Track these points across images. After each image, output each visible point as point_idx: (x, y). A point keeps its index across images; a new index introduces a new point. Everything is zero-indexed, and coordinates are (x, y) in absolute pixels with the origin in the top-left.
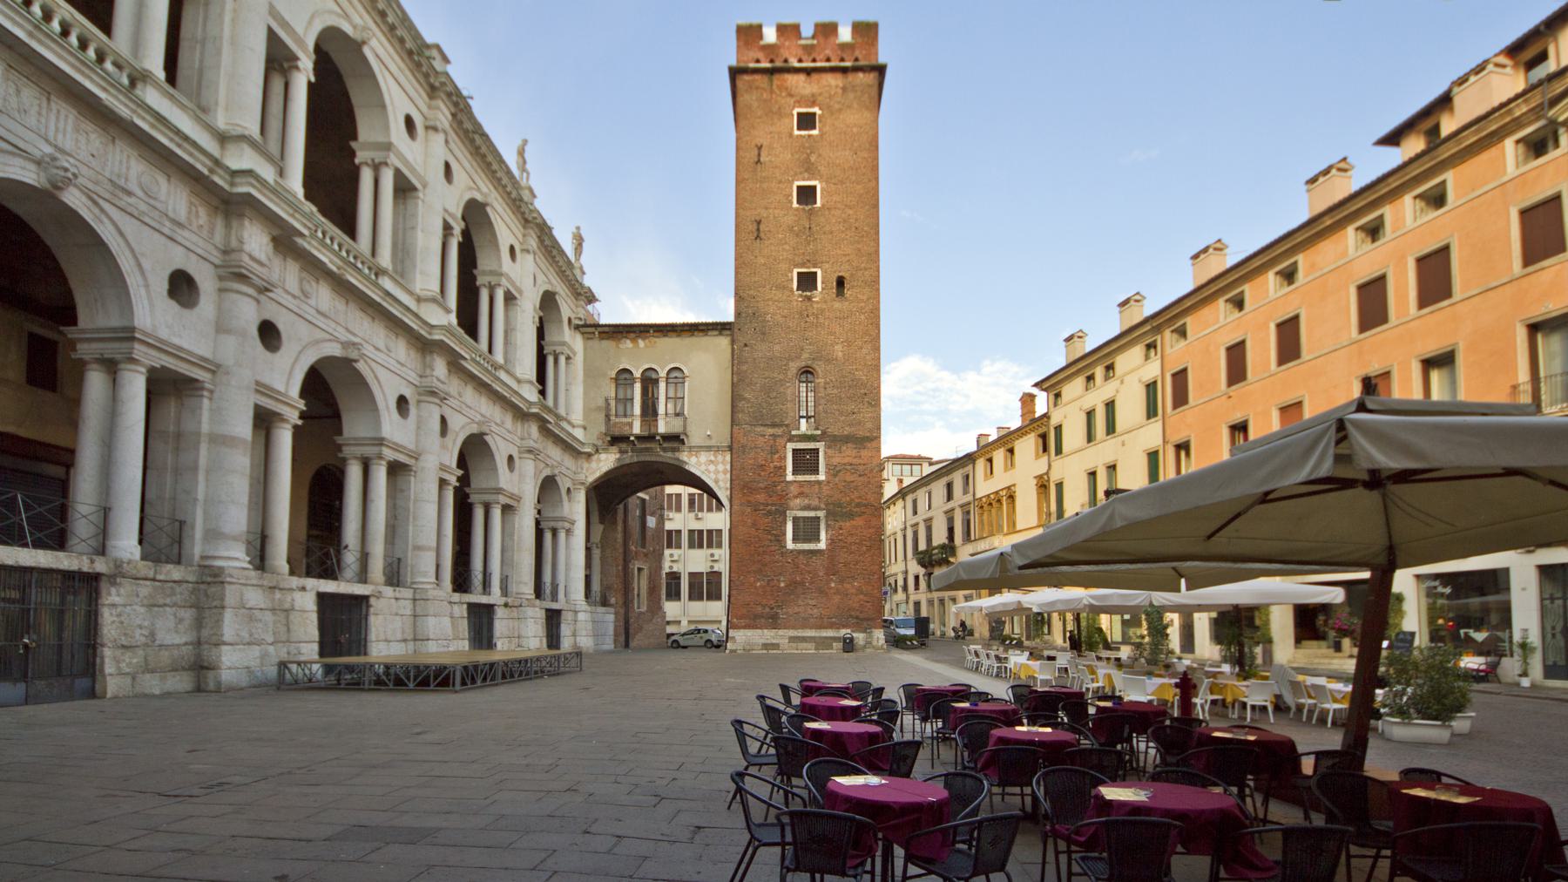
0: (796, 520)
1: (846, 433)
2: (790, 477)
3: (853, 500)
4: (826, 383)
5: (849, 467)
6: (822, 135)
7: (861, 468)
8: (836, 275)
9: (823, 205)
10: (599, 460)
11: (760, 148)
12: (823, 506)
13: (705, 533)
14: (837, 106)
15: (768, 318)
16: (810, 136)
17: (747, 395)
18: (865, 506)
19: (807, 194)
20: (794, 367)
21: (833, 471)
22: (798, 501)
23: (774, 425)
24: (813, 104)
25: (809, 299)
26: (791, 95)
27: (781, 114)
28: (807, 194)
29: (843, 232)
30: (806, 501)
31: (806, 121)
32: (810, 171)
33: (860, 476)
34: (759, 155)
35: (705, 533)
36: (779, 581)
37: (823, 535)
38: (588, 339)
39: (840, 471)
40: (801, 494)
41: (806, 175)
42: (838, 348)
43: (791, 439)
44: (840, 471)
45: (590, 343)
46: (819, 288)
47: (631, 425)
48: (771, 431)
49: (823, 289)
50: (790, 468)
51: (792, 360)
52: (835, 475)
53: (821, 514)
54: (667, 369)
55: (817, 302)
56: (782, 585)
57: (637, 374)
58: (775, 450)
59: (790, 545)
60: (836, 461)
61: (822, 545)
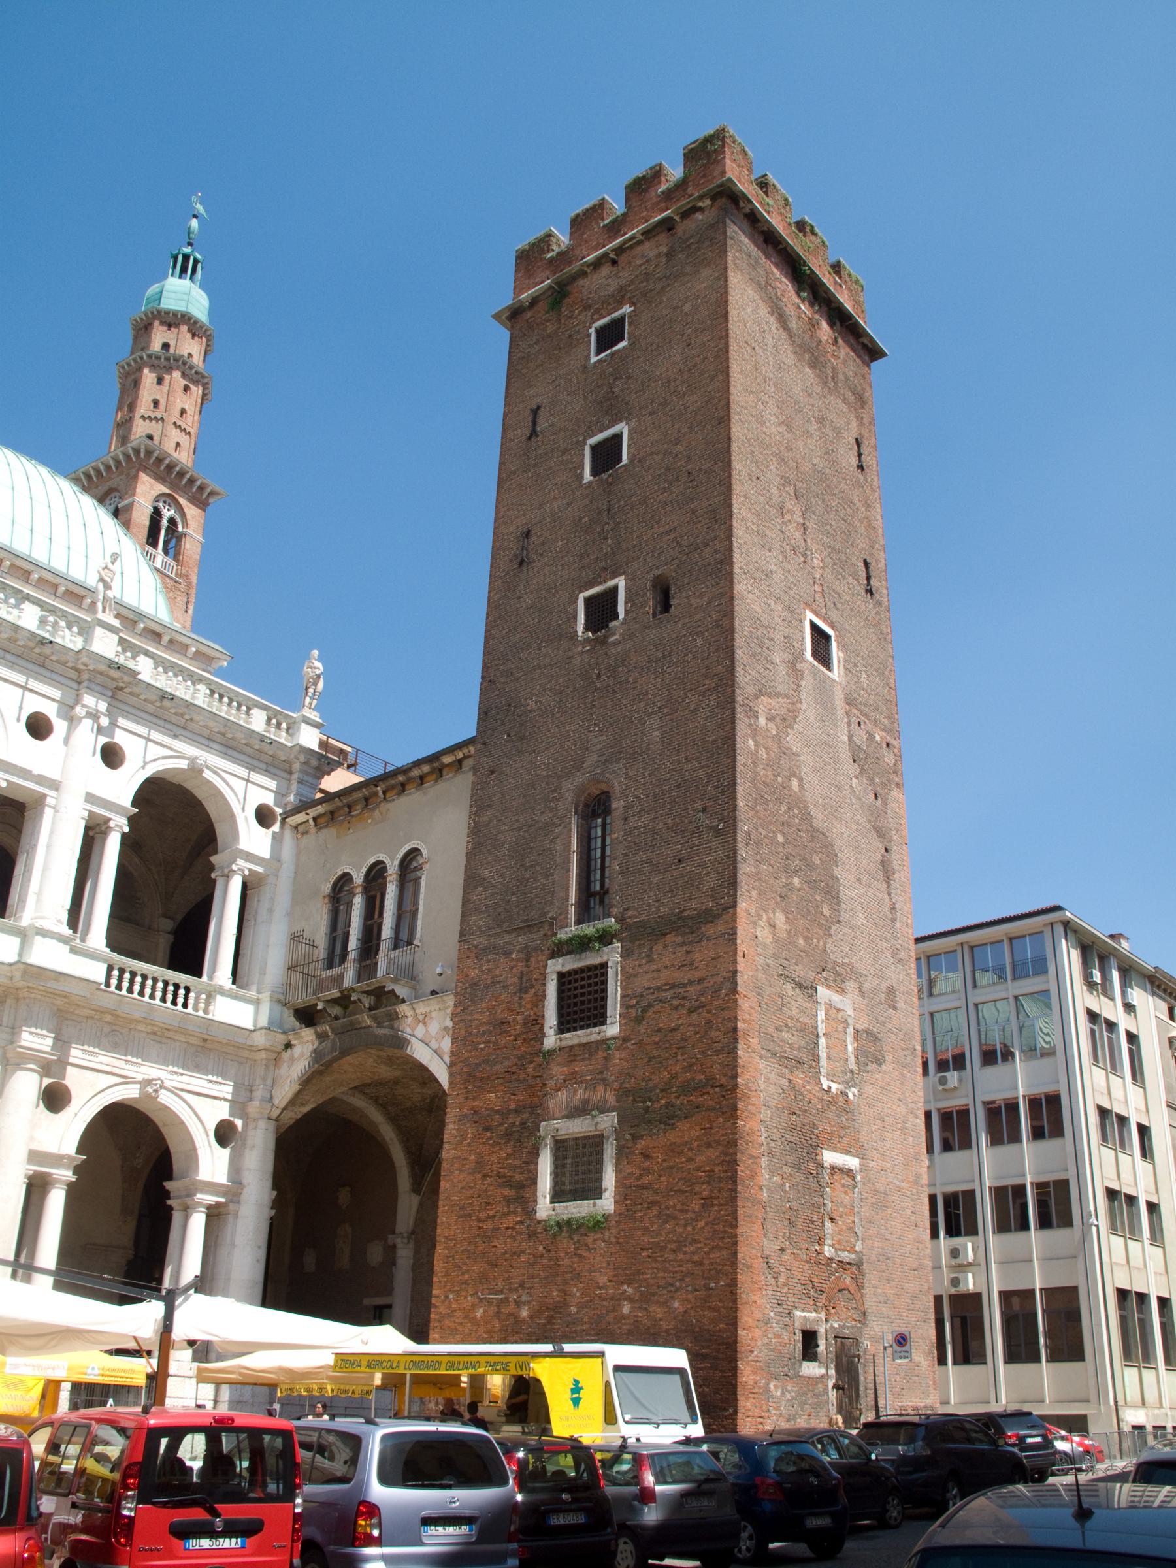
0: (560, 1146)
1: (663, 911)
2: (551, 1040)
3: (673, 1077)
4: (627, 807)
5: (668, 994)
6: (632, 345)
7: (693, 990)
8: (650, 576)
9: (631, 460)
10: (292, 1060)
11: (535, 412)
12: (611, 1100)
13: (1010, 1189)
14: (659, 286)
15: (532, 704)
16: (612, 355)
17: (485, 874)
18: (701, 1089)
19: (607, 454)
20: (569, 789)
21: (635, 1013)
22: (562, 1097)
23: (529, 927)
24: (620, 304)
25: (603, 642)
26: (587, 308)
27: (576, 340)
28: (607, 454)
29: (665, 490)
30: (580, 1094)
31: (609, 336)
32: (612, 410)
33: (691, 1011)
34: (534, 423)
35: (1010, 1189)
36: (518, 1304)
37: (609, 1179)
38: (303, 834)
39: (650, 1005)
40: (571, 1079)
41: (606, 420)
42: (654, 722)
43: (560, 950)
44: (650, 1005)
45: (305, 840)
46: (622, 615)
47: (341, 977)
48: (522, 939)
49: (627, 612)
50: (551, 1019)
51: (568, 775)
52: (639, 1020)
53: (607, 1122)
54: (400, 856)
55: (616, 643)
56: (524, 1313)
57: (358, 879)
58: (530, 985)
59: (544, 1207)
60: (643, 982)
61: (607, 1203)
